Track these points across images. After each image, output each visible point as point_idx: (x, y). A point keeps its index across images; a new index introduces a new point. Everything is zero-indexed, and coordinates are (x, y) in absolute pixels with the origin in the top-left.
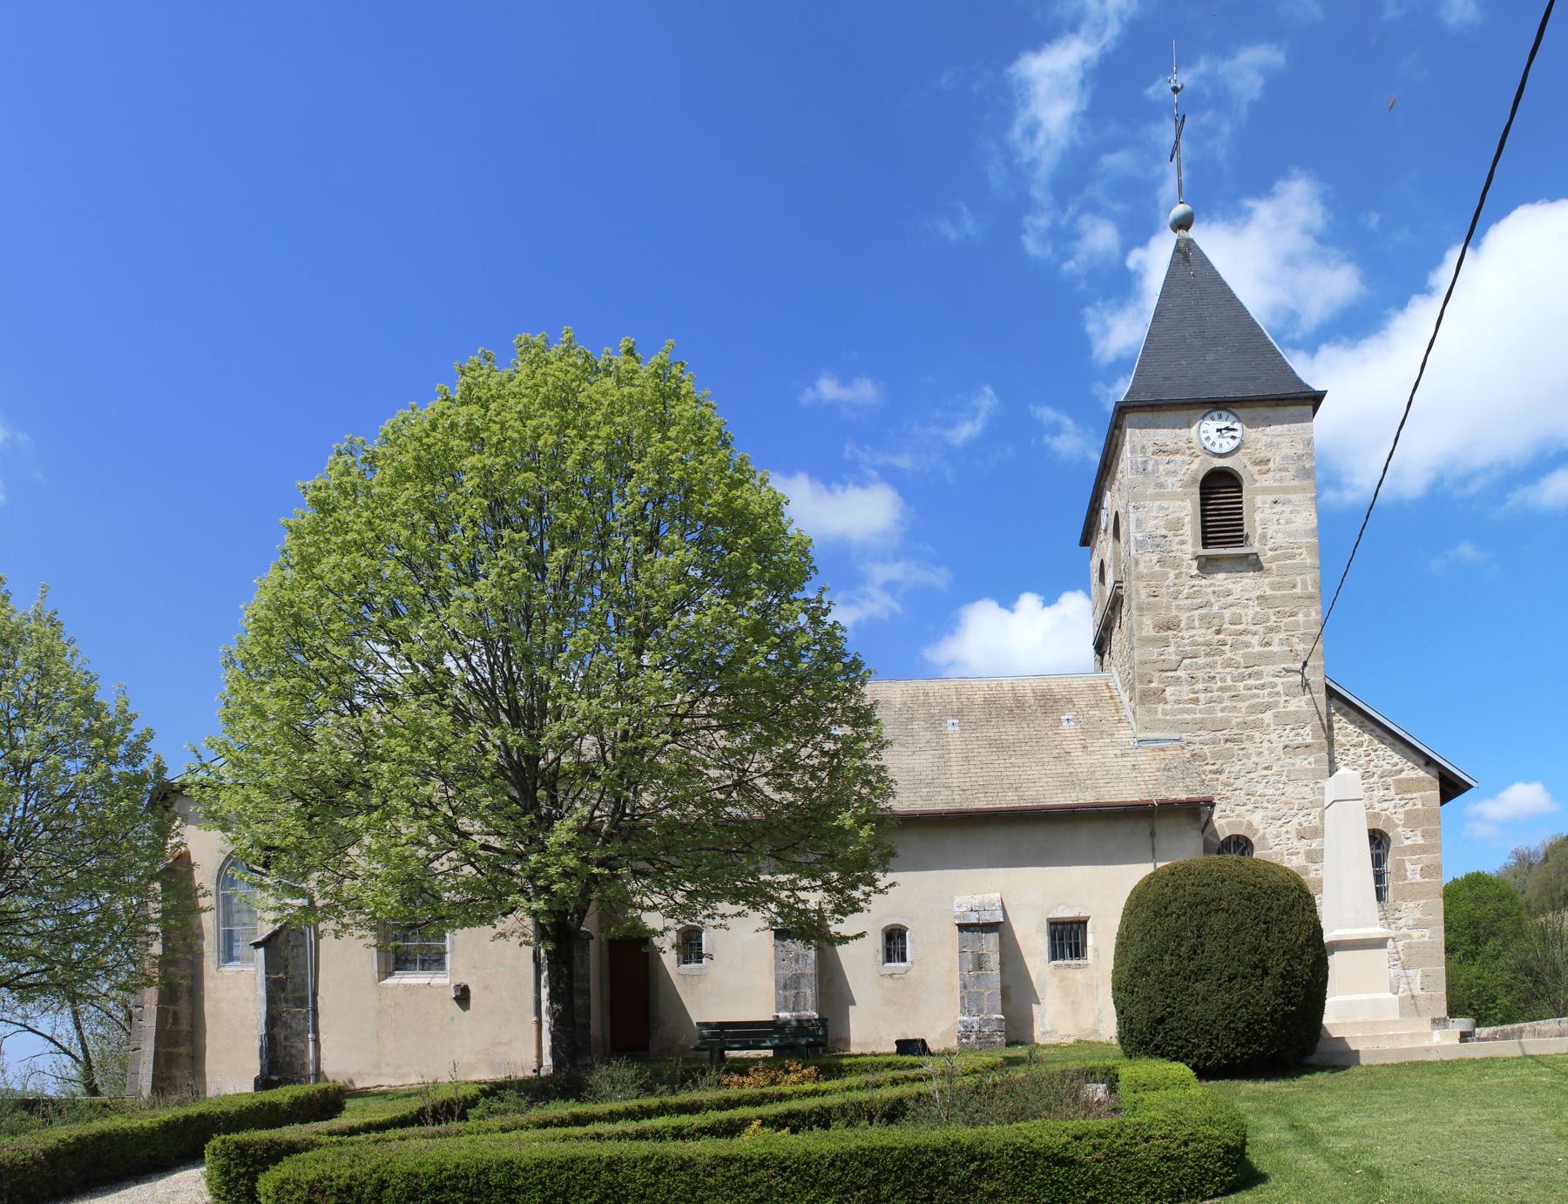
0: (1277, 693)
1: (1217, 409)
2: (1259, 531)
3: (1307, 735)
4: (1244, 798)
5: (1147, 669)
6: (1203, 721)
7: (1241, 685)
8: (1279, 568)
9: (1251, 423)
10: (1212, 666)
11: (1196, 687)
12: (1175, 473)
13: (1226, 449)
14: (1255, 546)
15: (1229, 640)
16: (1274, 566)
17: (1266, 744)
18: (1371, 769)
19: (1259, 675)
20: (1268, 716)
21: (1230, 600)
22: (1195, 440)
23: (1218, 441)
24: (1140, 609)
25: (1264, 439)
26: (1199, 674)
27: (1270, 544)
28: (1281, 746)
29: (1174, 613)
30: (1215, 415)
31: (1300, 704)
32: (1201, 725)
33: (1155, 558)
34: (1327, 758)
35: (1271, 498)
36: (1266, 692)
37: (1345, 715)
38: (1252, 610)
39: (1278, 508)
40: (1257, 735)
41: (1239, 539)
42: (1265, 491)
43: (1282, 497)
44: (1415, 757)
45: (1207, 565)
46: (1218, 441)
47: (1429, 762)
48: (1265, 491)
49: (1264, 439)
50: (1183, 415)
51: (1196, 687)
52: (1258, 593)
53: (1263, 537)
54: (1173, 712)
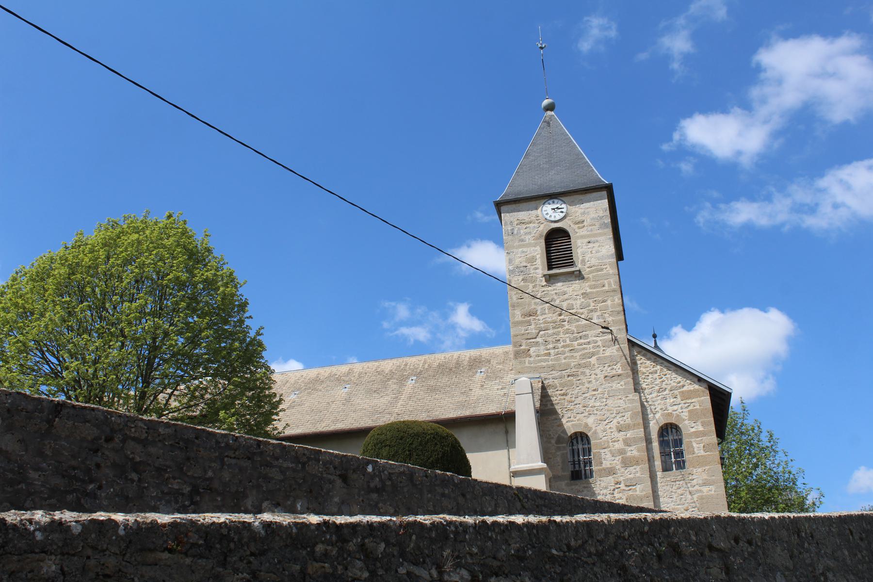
0: (598, 346)
1: (551, 199)
2: (581, 258)
3: (618, 369)
4: (582, 409)
5: (518, 339)
6: (553, 365)
7: (576, 343)
8: (594, 277)
9: (571, 204)
10: (558, 334)
11: (548, 347)
12: (530, 233)
13: (558, 218)
14: (579, 266)
15: (567, 318)
16: (590, 276)
17: (593, 376)
18: (664, 386)
19: (586, 336)
20: (593, 360)
21: (566, 296)
22: (540, 215)
23: (553, 215)
24: (513, 306)
25: (580, 211)
26: (550, 339)
27: (588, 265)
28: (602, 376)
29: (533, 306)
30: (551, 201)
31: (612, 351)
32: (553, 368)
33: (521, 278)
34: (632, 381)
35: (587, 240)
36: (591, 346)
37: (644, 355)
38: (580, 301)
39: (591, 245)
40: (587, 371)
41: (572, 264)
42: (582, 237)
43: (593, 239)
44: (691, 377)
45: (550, 279)
46: (553, 215)
47: (700, 380)
48: (582, 237)
49: (580, 211)
50: (533, 204)
51: (548, 347)
52: (583, 291)
53: (583, 261)
54: (535, 362)
